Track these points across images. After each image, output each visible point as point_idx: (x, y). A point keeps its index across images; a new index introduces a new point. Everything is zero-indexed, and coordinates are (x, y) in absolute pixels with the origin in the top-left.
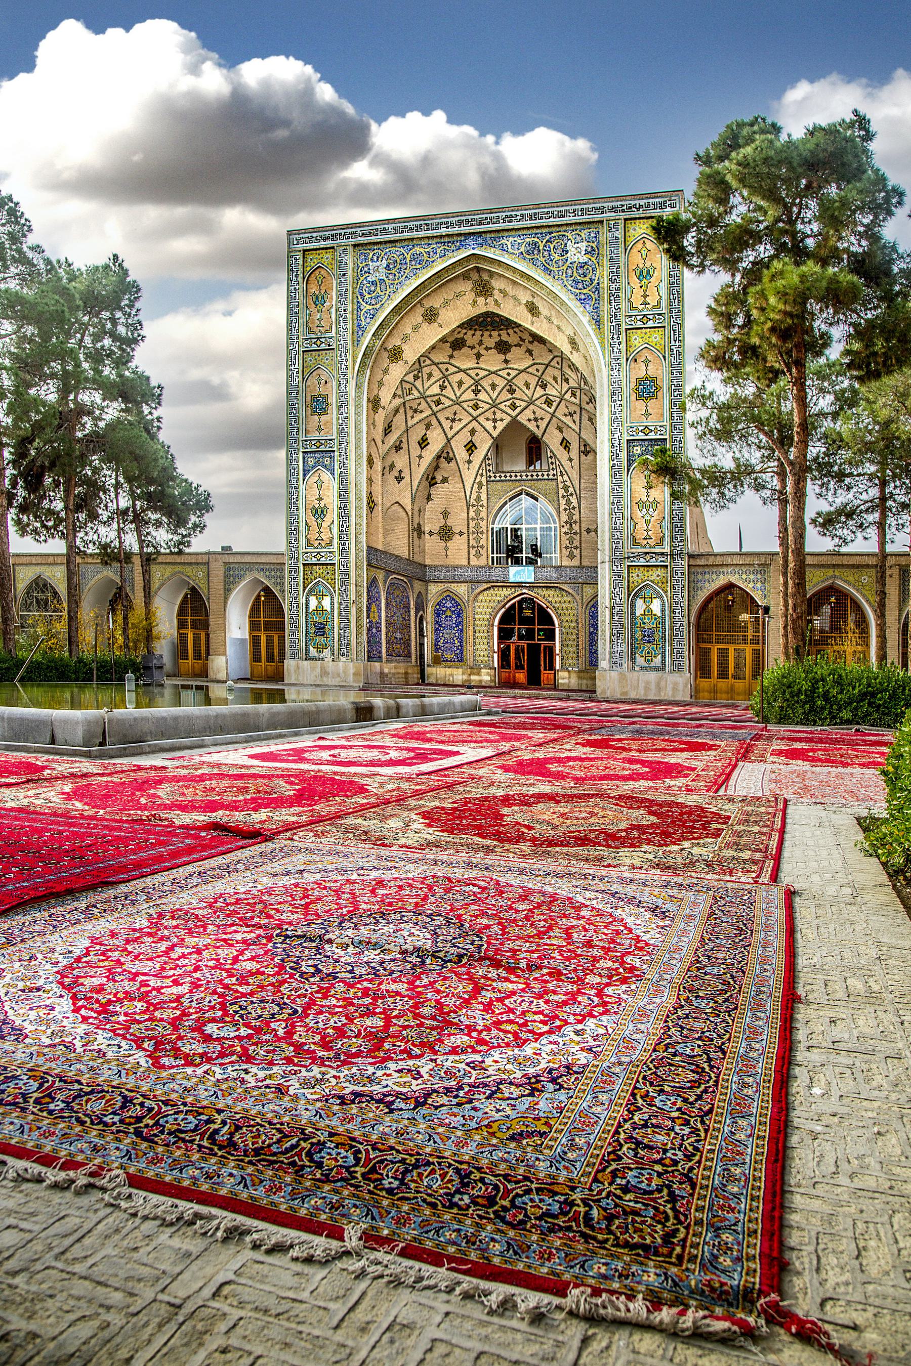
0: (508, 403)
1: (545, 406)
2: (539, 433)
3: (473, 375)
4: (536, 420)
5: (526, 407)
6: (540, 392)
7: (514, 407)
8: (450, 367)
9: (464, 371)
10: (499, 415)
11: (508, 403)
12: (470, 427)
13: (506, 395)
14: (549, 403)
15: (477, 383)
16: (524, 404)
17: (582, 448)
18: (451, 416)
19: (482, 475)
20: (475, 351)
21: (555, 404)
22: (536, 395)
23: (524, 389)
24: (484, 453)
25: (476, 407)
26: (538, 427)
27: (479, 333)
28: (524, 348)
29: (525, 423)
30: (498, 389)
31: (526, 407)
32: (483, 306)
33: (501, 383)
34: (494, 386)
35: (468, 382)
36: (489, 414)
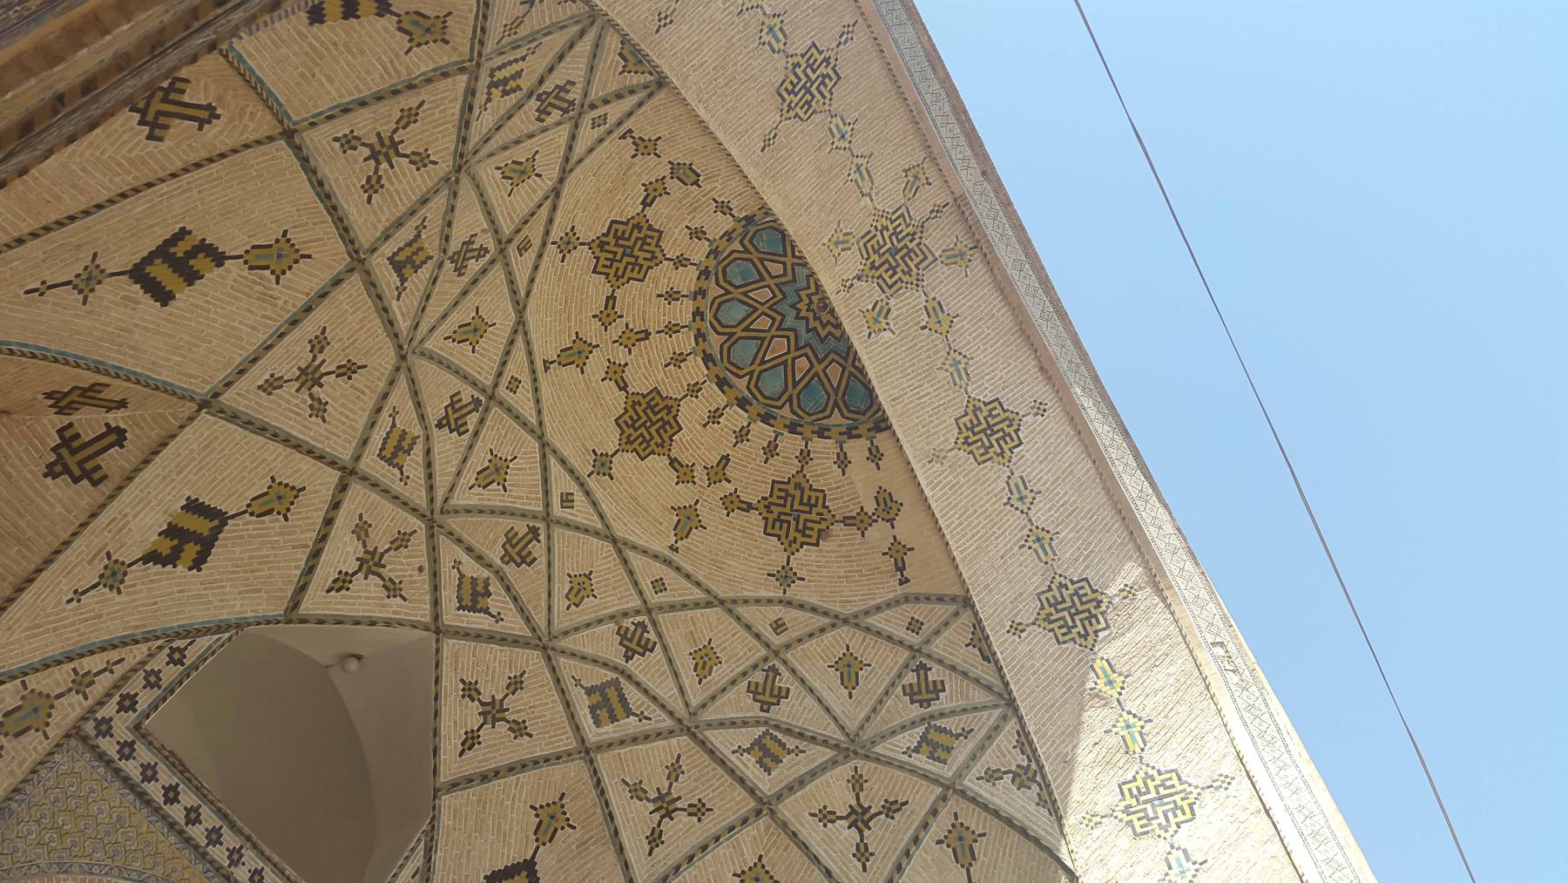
0: (471, 568)
2: (451, 765)
3: (511, 370)
4: (493, 712)
5: (515, 642)
9: (521, 322)
10: (406, 565)
11: (471, 568)
13: (490, 538)
15: (487, 399)
16: (513, 624)
19: (82, 683)
20: (592, 330)
21: (630, 725)
22: (580, 642)
23: (562, 587)
24: (199, 615)
25: (395, 452)
26: (471, 740)
27: (683, 311)
28: (684, 495)
29: (450, 685)
30: (493, 497)
31: (515, 642)
33: (522, 490)
34: (495, 473)
35: (481, 362)
36: (388, 520)
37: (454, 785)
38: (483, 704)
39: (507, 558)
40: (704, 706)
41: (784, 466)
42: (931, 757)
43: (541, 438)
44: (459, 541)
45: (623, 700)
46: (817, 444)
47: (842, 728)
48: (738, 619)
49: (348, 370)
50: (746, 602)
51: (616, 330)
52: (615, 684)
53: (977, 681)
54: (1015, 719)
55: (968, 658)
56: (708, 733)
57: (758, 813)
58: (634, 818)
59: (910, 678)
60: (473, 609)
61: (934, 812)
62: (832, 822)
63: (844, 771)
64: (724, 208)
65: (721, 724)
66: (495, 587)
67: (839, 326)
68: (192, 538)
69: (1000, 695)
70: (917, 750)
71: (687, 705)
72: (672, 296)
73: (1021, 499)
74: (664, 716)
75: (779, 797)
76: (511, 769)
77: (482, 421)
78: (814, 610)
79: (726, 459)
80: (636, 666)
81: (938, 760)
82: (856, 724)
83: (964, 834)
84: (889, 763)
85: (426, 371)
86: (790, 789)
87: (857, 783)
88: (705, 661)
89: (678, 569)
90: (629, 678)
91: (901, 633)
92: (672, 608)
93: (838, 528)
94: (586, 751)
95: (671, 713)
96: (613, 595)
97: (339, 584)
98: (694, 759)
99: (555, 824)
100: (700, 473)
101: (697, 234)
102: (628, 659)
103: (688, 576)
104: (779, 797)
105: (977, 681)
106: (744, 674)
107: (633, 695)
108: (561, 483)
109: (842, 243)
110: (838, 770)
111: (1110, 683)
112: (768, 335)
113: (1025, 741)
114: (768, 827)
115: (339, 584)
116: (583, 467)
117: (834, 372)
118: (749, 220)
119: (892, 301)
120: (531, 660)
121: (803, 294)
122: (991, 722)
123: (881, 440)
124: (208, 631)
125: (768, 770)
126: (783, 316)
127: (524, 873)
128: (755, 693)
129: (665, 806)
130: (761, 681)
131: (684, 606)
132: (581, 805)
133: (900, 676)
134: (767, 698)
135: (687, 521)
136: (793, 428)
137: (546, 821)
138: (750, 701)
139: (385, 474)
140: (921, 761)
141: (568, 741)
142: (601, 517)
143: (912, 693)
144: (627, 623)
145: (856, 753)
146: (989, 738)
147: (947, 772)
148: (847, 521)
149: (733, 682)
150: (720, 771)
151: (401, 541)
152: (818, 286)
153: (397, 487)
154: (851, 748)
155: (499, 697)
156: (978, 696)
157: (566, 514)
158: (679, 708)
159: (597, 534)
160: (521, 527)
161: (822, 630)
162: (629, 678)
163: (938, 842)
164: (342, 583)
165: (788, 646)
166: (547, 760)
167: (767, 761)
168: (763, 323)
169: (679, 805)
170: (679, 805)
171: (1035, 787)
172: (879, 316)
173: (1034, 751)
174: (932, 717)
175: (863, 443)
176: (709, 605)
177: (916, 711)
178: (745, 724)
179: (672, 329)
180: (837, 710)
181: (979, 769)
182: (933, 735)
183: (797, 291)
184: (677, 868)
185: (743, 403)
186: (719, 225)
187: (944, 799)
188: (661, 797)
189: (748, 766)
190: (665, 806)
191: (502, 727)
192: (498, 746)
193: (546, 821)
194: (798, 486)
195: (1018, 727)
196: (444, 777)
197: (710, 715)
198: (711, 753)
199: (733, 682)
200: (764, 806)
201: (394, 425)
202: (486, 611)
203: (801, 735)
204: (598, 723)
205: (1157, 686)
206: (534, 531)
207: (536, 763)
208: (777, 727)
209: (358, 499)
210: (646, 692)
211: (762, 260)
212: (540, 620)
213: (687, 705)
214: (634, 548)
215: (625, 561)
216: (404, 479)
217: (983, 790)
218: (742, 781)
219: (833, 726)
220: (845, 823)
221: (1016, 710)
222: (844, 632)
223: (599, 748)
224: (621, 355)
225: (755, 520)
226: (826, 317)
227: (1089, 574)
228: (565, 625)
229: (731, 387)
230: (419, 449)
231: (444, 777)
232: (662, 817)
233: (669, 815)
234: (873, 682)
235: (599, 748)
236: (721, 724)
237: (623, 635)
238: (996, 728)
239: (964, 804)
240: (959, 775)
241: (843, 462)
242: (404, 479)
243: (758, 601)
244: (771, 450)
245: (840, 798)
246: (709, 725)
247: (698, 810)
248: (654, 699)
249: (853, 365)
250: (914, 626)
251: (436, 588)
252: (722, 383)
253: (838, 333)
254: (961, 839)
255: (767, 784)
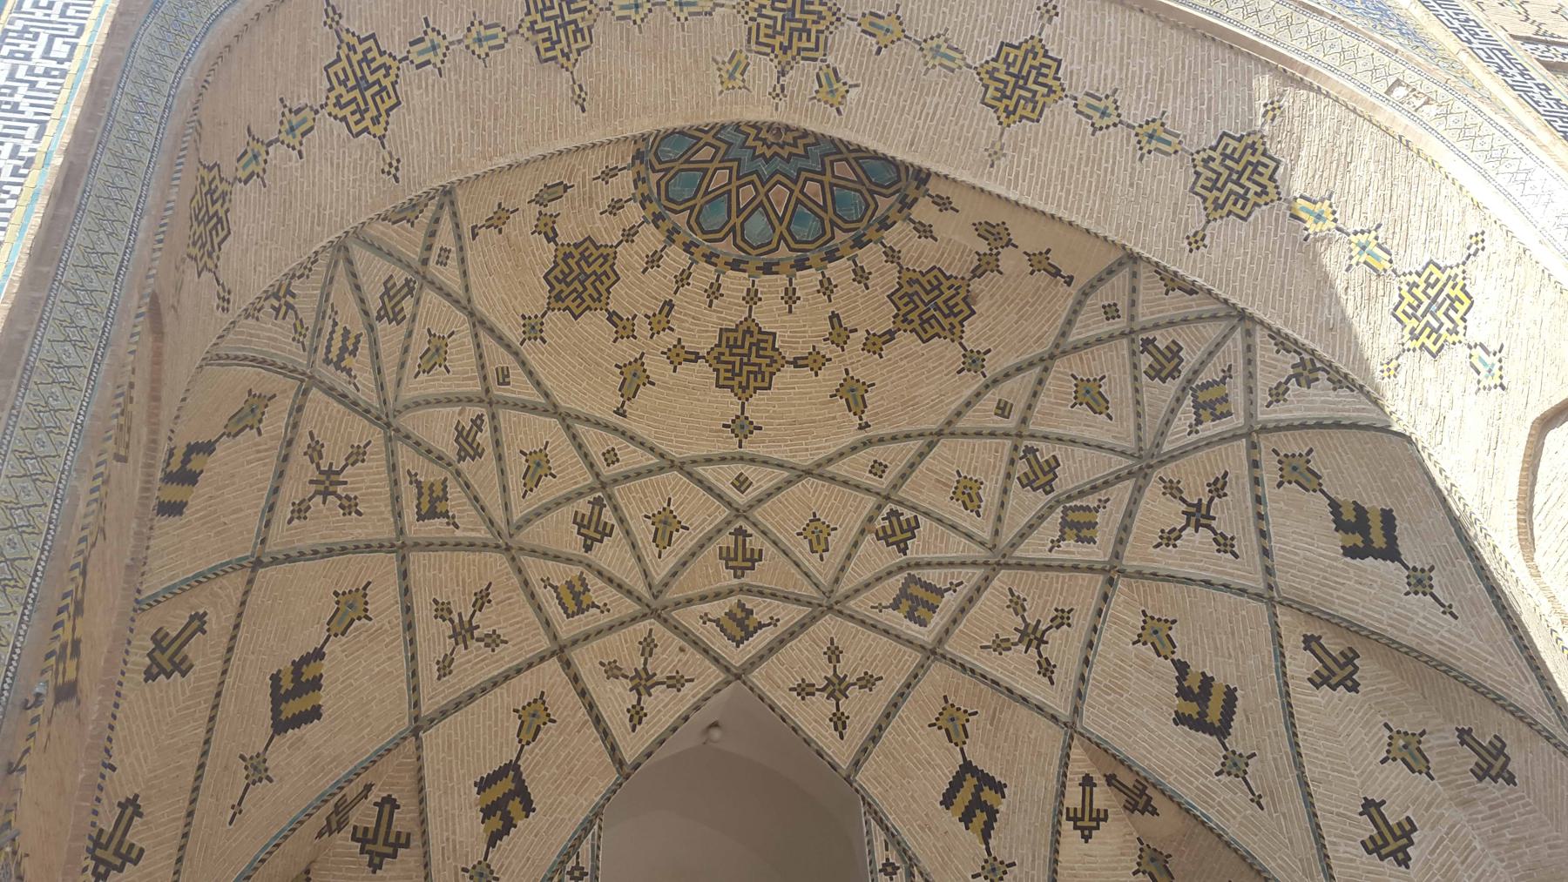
0: (718, 609)
1: (897, 620)
2: (841, 752)
3: (596, 452)
5: (803, 626)
6: (876, 556)
7: (741, 626)
8: (517, 374)
10: (670, 657)
11: (718, 609)
12: (524, 689)
13: (712, 573)
14: (917, 601)
16: (790, 614)
17: (1074, 798)
18: (462, 607)
21: (950, 601)
23: (801, 550)
25: (576, 599)
26: (839, 722)
27: (676, 258)
28: (831, 377)
29: (785, 701)
30: (683, 543)
31: (803, 626)
32: (762, 99)
33: (700, 513)
34: (666, 526)
35: (570, 473)
36: (624, 647)
37: (856, 764)
38: (823, 690)
39: (739, 572)
40: (997, 532)
41: (885, 278)
42: (1216, 417)
43: (672, 465)
44: (689, 601)
45: (928, 587)
46: (890, 237)
47: (1123, 453)
48: (965, 434)
49: (482, 599)
50: (959, 414)
51: (642, 328)
52: (912, 579)
53: (1199, 319)
54: (1258, 327)
55: (1176, 304)
56: (1017, 553)
57: (1111, 582)
58: (1016, 669)
59: (1145, 361)
60: (749, 635)
61: (1255, 464)
62: (1179, 537)
63: (1154, 488)
64: (609, 174)
65: (1022, 536)
66: (750, 602)
67: (805, 134)
68: (505, 799)
69: (1228, 316)
70: (1199, 422)
71: (982, 544)
72: (654, 260)
73: (1104, 114)
74: (970, 571)
75: (1117, 555)
76: (888, 715)
77: (616, 509)
78: (1019, 369)
79: (834, 317)
80: (915, 550)
81: (1223, 415)
82: (1133, 438)
83: (1295, 462)
84: (1184, 452)
85: (533, 535)
86: (1121, 541)
87: (1172, 489)
88: (967, 494)
89: (881, 440)
90: (918, 565)
91: (1106, 328)
92: (904, 477)
93: (976, 285)
94: (933, 653)
95: (974, 564)
96: (849, 514)
97: (636, 718)
98: (1024, 583)
99: (958, 723)
100: (826, 349)
101: (616, 207)
102: (904, 551)
103: (894, 438)
104: (1117, 555)
105: (1199, 319)
106: (1008, 476)
107: (932, 576)
108: (721, 476)
109: (737, 67)
110: (1147, 493)
111: (1319, 217)
112: (762, 197)
113: (1283, 342)
114: (1129, 586)
115: (636, 718)
116: (730, 446)
117: (842, 169)
118: (639, 156)
119: (830, 60)
120: (829, 626)
121: (750, 142)
122: (1240, 347)
123: (933, 187)
124: (580, 840)
125: (1092, 540)
126: (756, 172)
127: (968, 776)
128: (1030, 484)
129: (1033, 637)
130: (1027, 469)
131: (912, 466)
132: (965, 693)
133: (1135, 366)
134: (1043, 479)
135: (853, 394)
136: (859, 243)
137: (950, 726)
138: (1031, 494)
139: (582, 623)
140: (1210, 428)
141: (912, 658)
142: (780, 466)
143: (1156, 373)
144: (879, 523)
145: (1150, 467)
146: (1249, 362)
147: (1237, 421)
148: (977, 273)
149: (1005, 491)
150: (1052, 574)
151: (648, 646)
152: (755, 126)
153: (605, 619)
154: (1143, 465)
155: (830, 674)
156: (1212, 331)
157: (752, 494)
158: (979, 553)
159: (789, 482)
160: (727, 540)
161: (1040, 382)
162: (918, 565)
163: (1280, 485)
164: (637, 716)
165: (1024, 421)
166: (908, 686)
167: (1085, 533)
168: (747, 193)
169: (1042, 627)
170: (1042, 627)
171: (1321, 375)
172: (831, 86)
173: (1296, 342)
174: (1189, 381)
175: (924, 201)
176: (931, 445)
177: (1172, 386)
178: (1042, 518)
179: (683, 279)
180: (1108, 440)
181: (1262, 396)
182: (1203, 397)
183: (743, 146)
184: (1082, 678)
185: (801, 265)
186: (623, 184)
187: (1254, 446)
188: (1023, 634)
189: (1073, 550)
190: (1033, 637)
191: (853, 692)
192: (863, 708)
193: (950, 726)
194: (911, 282)
195: (1266, 332)
196: (844, 764)
197: (1008, 535)
198: (1032, 566)
199: (1005, 491)
200: (1111, 573)
201: (555, 588)
202: (761, 626)
203: (1094, 489)
204: (923, 624)
205: (1364, 183)
206: (740, 532)
207: (902, 695)
208: (1070, 498)
209: (586, 660)
210: (940, 564)
211: (687, 161)
212: (807, 590)
213: (982, 544)
214: (830, 461)
215: (833, 479)
216: (604, 609)
217: (1280, 413)
218: (1075, 568)
219: (1115, 458)
220: (1190, 530)
221: (1252, 318)
222: (1059, 365)
223: (940, 641)
224: (668, 339)
225: (906, 339)
226: (789, 138)
227: (1224, 127)
228: (831, 575)
229: (777, 264)
230: (591, 579)
231: (844, 764)
232: (1038, 648)
233: (1041, 641)
234: (1118, 390)
235: (940, 641)
236: (1022, 536)
237: (883, 536)
238: (1249, 348)
239: (1274, 437)
240: (1250, 415)
241: (925, 231)
242: (604, 609)
243: (968, 404)
244: (861, 276)
245: (1170, 513)
246: (1013, 545)
247: (1062, 618)
248: (951, 564)
249: (850, 151)
250: (1111, 312)
251: (706, 651)
252: (768, 269)
253: (811, 140)
254: (1295, 469)
255: (1098, 553)
